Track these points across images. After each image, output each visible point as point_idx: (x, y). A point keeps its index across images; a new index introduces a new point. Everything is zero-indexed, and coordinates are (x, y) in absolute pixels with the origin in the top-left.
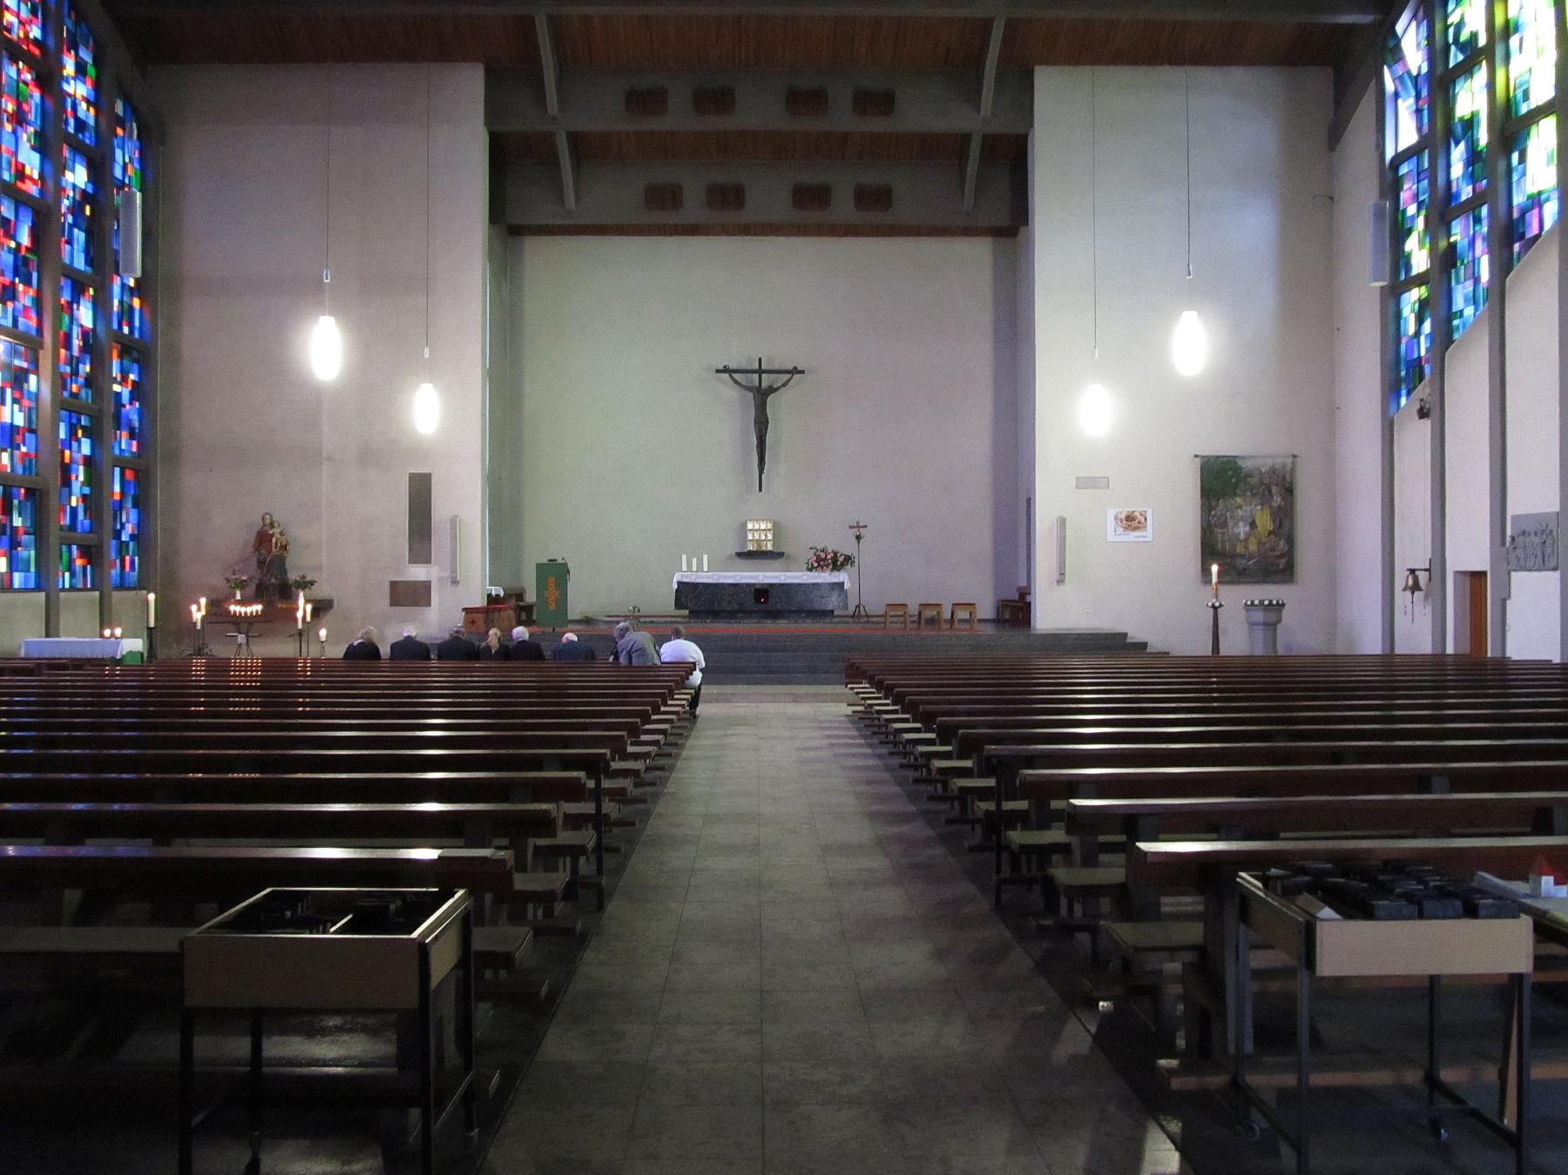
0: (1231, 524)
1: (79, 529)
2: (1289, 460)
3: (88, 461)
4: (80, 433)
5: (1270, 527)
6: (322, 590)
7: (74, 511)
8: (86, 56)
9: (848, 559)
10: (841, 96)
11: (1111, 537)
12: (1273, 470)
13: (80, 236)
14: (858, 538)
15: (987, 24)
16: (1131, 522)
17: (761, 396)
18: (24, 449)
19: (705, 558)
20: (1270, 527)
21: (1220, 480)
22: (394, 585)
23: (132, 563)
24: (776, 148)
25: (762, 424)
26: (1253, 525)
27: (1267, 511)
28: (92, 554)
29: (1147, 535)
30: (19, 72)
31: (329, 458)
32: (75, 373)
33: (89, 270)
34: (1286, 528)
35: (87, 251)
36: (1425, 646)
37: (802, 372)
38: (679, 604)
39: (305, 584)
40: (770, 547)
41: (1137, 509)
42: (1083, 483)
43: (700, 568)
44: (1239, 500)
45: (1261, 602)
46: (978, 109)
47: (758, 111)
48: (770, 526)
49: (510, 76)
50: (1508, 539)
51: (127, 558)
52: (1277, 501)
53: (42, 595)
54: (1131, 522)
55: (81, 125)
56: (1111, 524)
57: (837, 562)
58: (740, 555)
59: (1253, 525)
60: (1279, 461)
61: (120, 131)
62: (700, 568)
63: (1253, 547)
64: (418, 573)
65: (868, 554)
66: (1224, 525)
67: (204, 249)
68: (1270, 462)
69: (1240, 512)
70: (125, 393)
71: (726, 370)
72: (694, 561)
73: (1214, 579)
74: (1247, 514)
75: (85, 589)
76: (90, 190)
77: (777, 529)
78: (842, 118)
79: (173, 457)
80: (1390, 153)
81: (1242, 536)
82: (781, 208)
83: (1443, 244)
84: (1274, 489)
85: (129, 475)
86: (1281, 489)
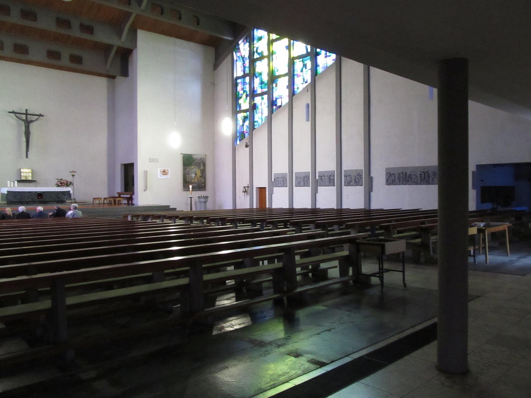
5: (200, 175)
10: (75, 24)
11: (159, 177)
12: (201, 159)
14: (73, 176)
15: (131, 14)
16: (164, 172)
17: (28, 123)
20: (200, 175)
21: (188, 161)
24: (43, 35)
25: (27, 134)
26: (196, 174)
29: (169, 176)
36: (247, 206)
37: (42, 116)
40: (30, 179)
41: (166, 169)
42: (152, 160)
47: (45, 23)
48: (30, 171)
50: (273, 180)
52: (202, 167)
54: (164, 172)
56: (159, 172)
57: (68, 184)
59: (196, 174)
60: (202, 156)
63: (196, 181)
65: (76, 181)
66: (189, 174)
68: (200, 156)
71: (13, 112)
73: (191, 189)
74: (195, 171)
77: (33, 173)
78: (76, 32)
80: (235, 76)
82: (42, 56)
83: (253, 103)
84: (201, 164)
86: (202, 164)
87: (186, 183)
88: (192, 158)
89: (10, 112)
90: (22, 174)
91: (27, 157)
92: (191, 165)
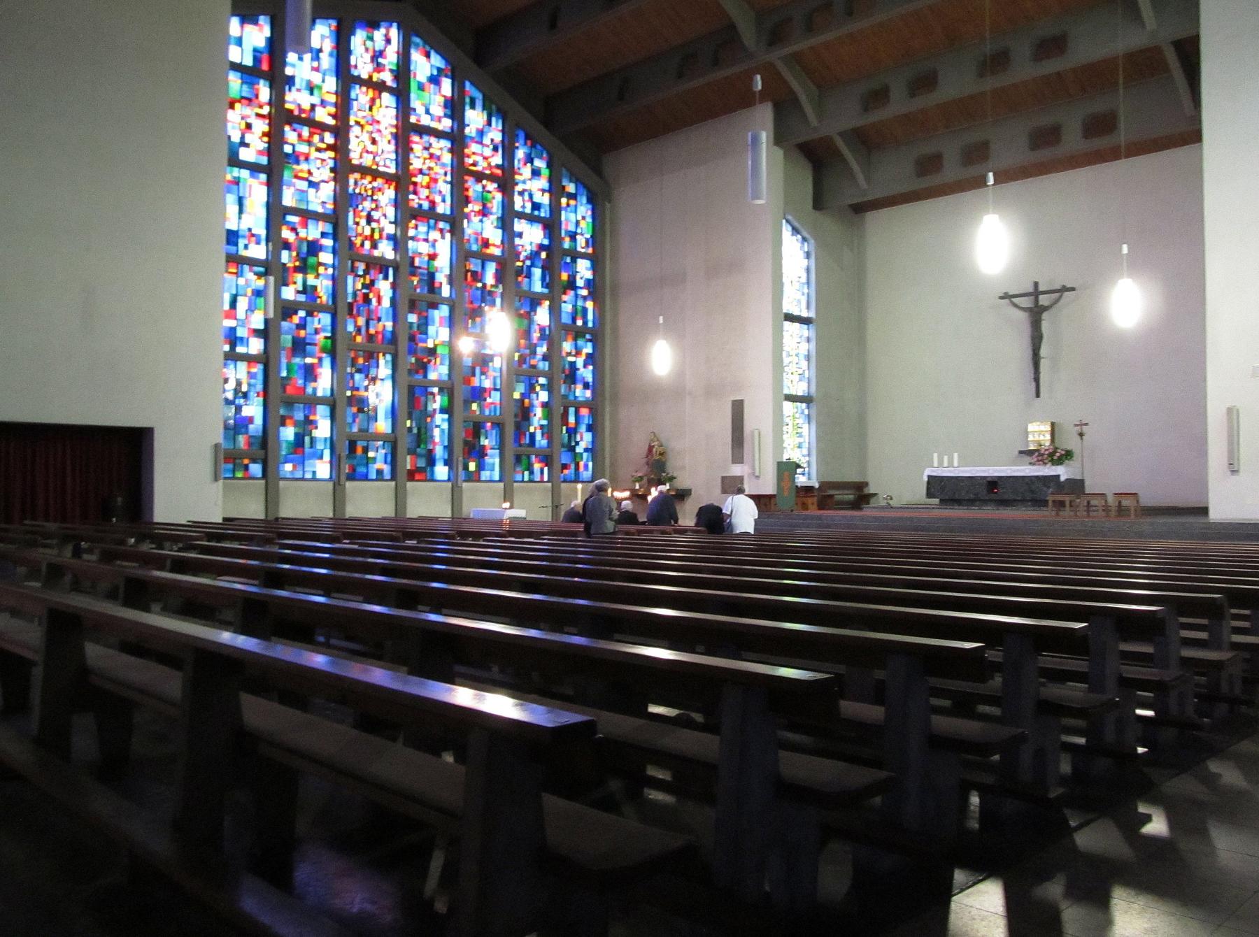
1: (537, 445)
3: (544, 405)
4: (538, 388)
6: (683, 482)
7: (533, 436)
8: (540, 164)
9: (1068, 455)
10: (1022, 50)
13: (537, 272)
14: (1081, 435)
17: (1036, 314)
18: (489, 400)
19: (956, 455)
22: (723, 478)
23: (586, 466)
28: (547, 460)
30: (484, 187)
31: (690, 394)
32: (534, 353)
33: (546, 291)
35: (543, 279)
37: (1073, 289)
38: (930, 494)
39: (671, 479)
43: (951, 464)
46: (1143, 25)
49: (785, 108)
51: (582, 464)
53: (502, 485)
55: (536, 206)
57: (1058, 456)
58: (1021, 452)
61: (572, 202)
62: (951, 464)
64: (736, 470)
67: (633, 262)
70: (580, 362)
71: (1006, 296)
72: (946, 458)
75: (542, 481)
76: (546, 242)
78: (1024, 70)
79: (615, 397)
85: (584, 412)
89: (1001, 298)
90: (1031, 438)
91: (1038, 395)
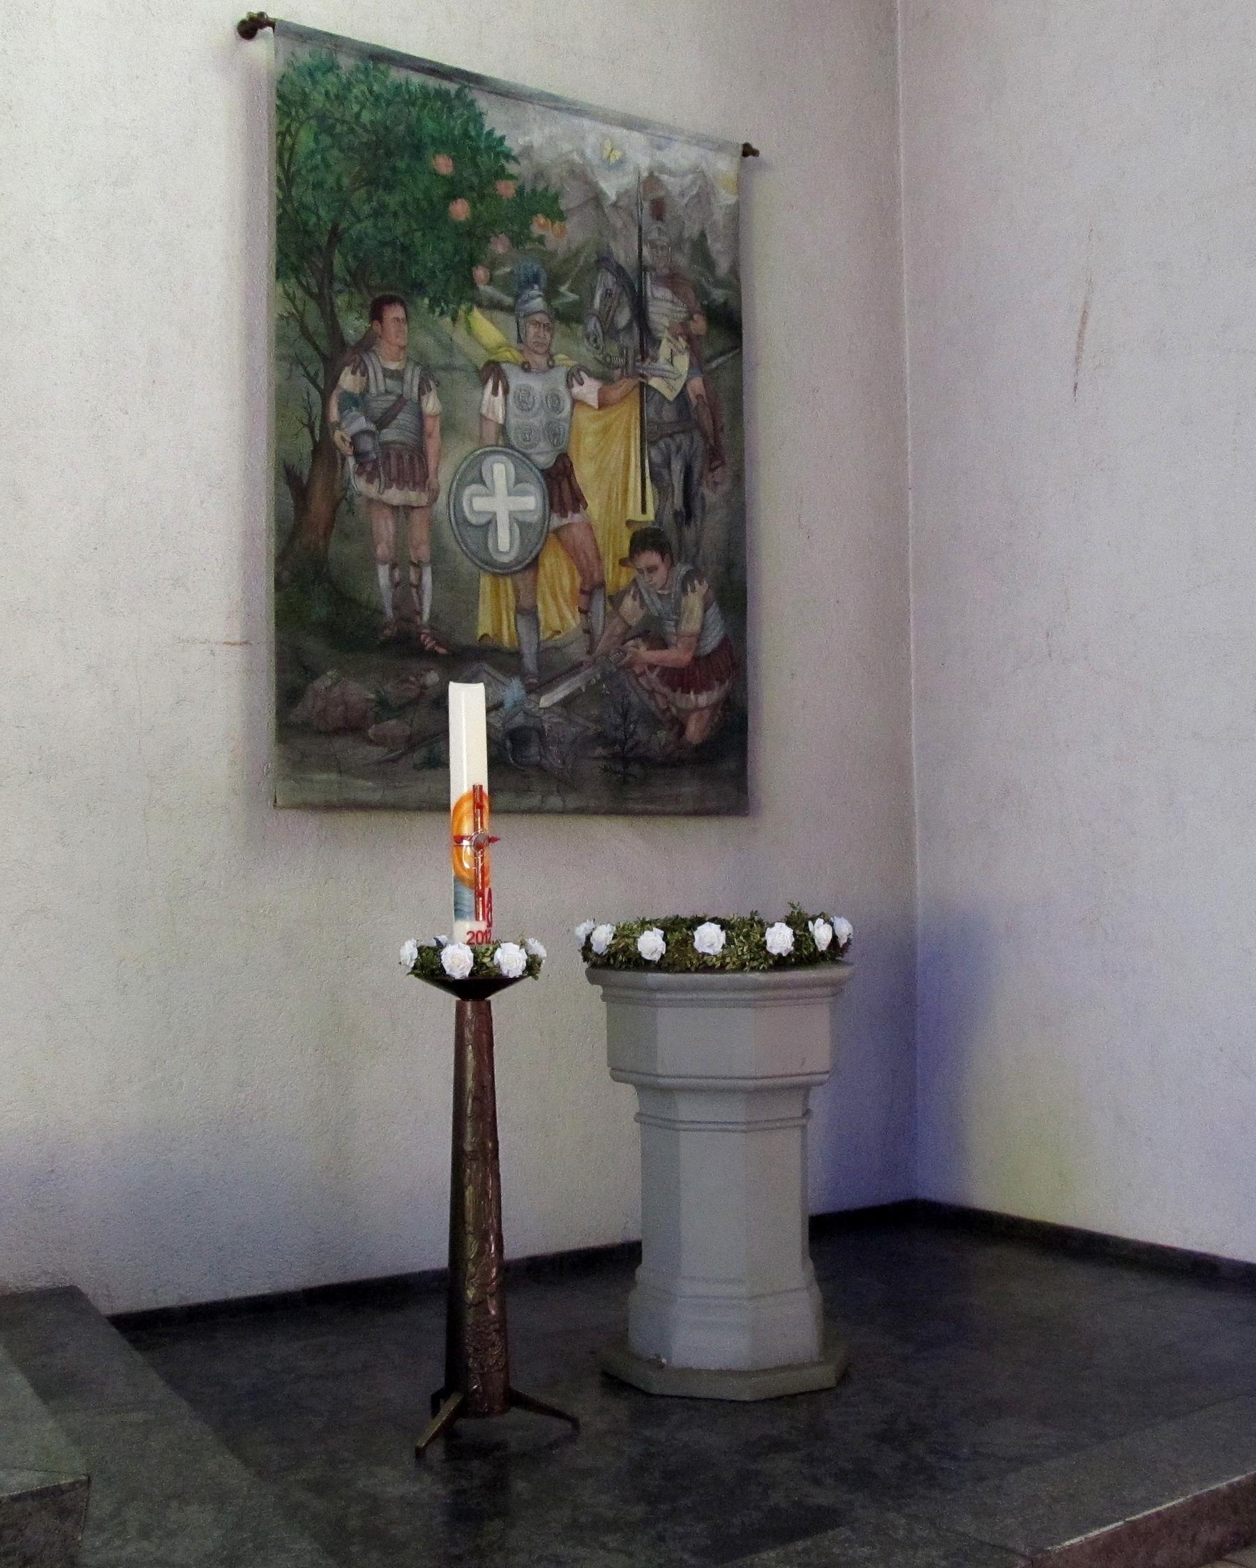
0: (444, 474)
2: (725, 166)
5: (640, 506)
12: (653, 201)
26: (560, 485)
27: (626, 417)
34: (712, 528)
44: (488, 331)
45: (744, 931)
59: (560, 485)
60: (680, 157)
63: (560, 615)
66: (411, 466)
69: (493, 404)
73: (468, 762)
81: (505, 543)
84: (664, 308)
86: (671, 299)
87: (344, 666)
88: (482, 159)
92: (457, 289)
